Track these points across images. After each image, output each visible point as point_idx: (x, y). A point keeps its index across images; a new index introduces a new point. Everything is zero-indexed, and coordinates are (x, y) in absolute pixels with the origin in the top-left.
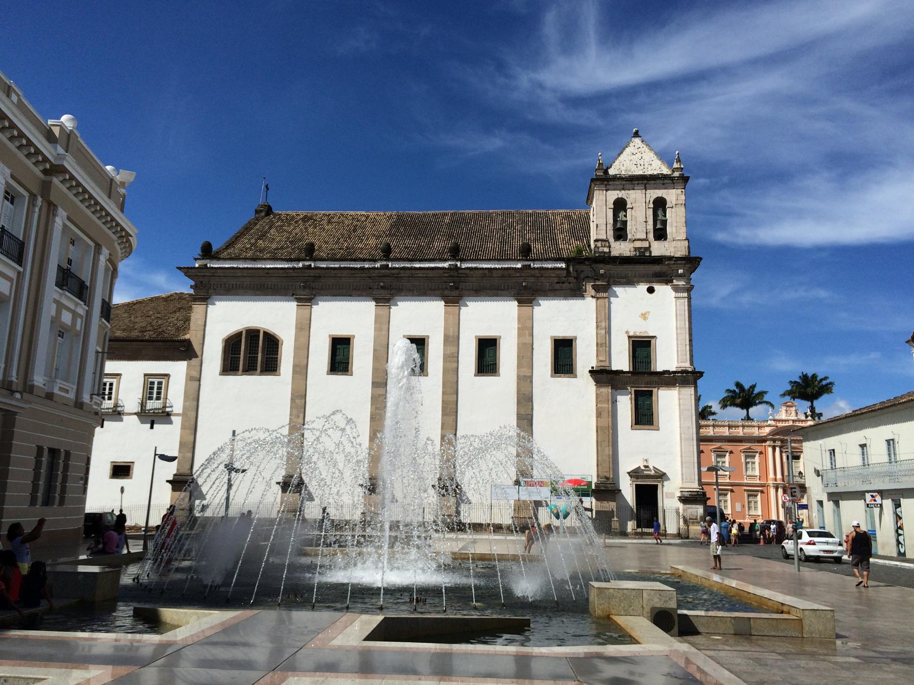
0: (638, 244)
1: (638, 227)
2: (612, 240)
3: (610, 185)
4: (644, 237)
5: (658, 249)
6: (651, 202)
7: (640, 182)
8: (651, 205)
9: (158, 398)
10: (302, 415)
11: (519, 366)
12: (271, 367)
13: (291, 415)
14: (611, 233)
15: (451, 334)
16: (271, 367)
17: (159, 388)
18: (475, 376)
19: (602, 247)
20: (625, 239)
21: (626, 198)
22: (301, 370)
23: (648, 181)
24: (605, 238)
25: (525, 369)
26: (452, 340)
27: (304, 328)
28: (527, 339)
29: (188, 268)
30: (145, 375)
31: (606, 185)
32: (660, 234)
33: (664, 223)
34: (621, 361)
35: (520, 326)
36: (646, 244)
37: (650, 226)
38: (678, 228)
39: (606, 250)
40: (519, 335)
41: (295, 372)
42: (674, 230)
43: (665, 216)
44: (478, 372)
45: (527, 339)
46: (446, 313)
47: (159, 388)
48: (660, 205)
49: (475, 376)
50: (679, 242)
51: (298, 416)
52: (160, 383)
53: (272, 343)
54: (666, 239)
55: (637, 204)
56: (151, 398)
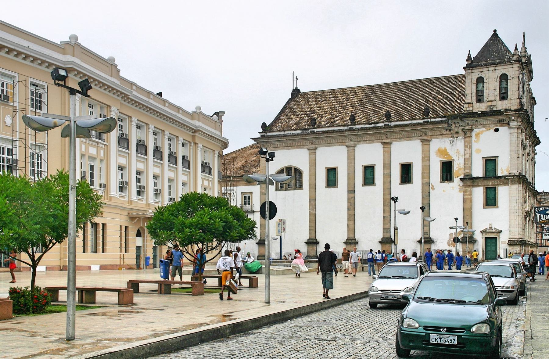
0: (490, 104)
1: (489, 93)
2: (475, 102)
3: (474, 69)
4: (493, 99)
5: (501, 105)
6: (498, 77)
7: (492, 66)
8: (498, 79)
9: (249, 204)
10: (315, 209)
11: (423, 178)
12: (299, 186)
13: (309, 209)
14: (474, 98)
15: (387, 163)
16: (299, 186)
17: (249, 199)
18: (400, 184)
19: (469, 107)
20: (483, 102)
21: (483, 76)
22: (313, 187)
23: (497, 65)
24: (470, 101)
25: (426, 180)
26: (387, 166)
27: (313, 164)
28: (426, 163)
29: (256, 138)
30: (242, 193)
31: (472, 70)
32: (504, 96)
33: (506, 89)
34: (478, 171)
35: (423, 156)
36: (494, 103)
37: (497, 92)
38: (514, 92)
39: (471, 109)
40: (423, 161)
41: (310, 188)
42: (512, 93)
43: (507, 85)
44: (402, 183)
45: (426, 163)
46: (384, 152)
47: (249, 199)
48: (504, 77)
49: (400, 184)
50: (514, 100)
51: (313, 210)
52: (249, 197)
53: (298, 172)
54: (507, 100)
55: (490, 80)
56: (245, 204)
